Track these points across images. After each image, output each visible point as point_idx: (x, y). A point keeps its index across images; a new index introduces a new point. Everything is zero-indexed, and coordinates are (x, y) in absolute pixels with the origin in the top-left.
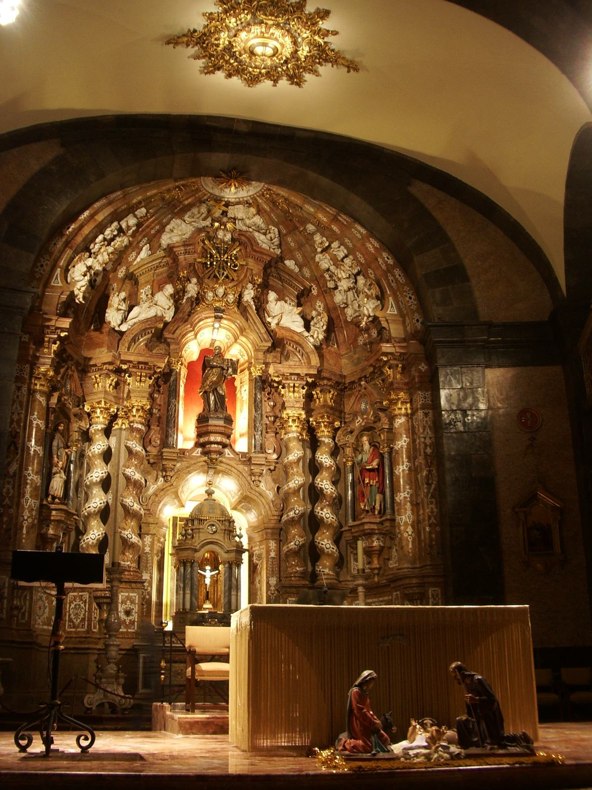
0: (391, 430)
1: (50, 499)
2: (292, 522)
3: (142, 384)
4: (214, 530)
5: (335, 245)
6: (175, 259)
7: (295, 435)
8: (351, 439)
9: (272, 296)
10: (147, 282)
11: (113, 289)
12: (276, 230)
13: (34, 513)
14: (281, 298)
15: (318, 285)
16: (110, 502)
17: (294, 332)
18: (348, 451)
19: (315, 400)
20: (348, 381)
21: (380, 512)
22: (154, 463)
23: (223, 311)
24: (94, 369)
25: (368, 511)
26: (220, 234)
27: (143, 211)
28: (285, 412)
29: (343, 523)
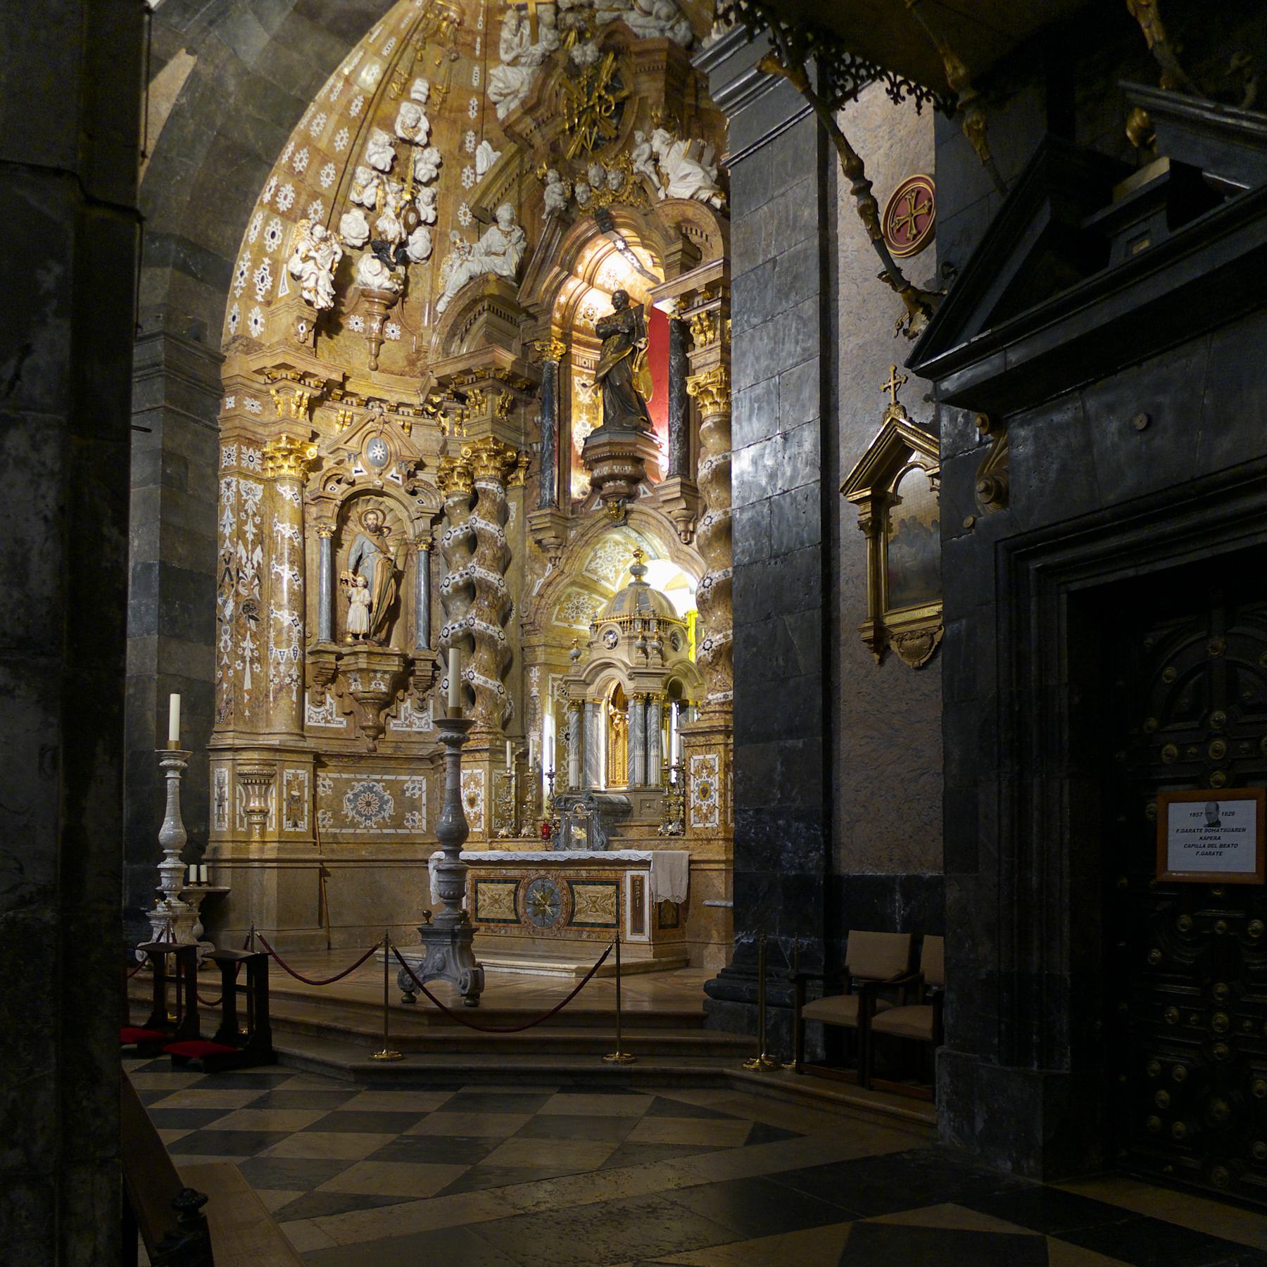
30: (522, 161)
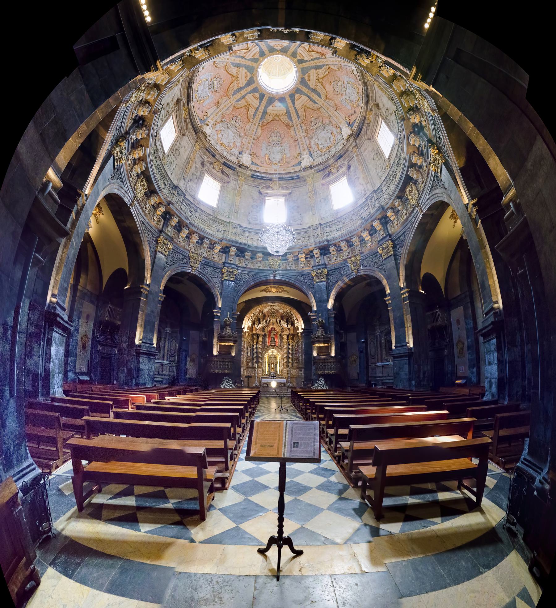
9: (282, 321)
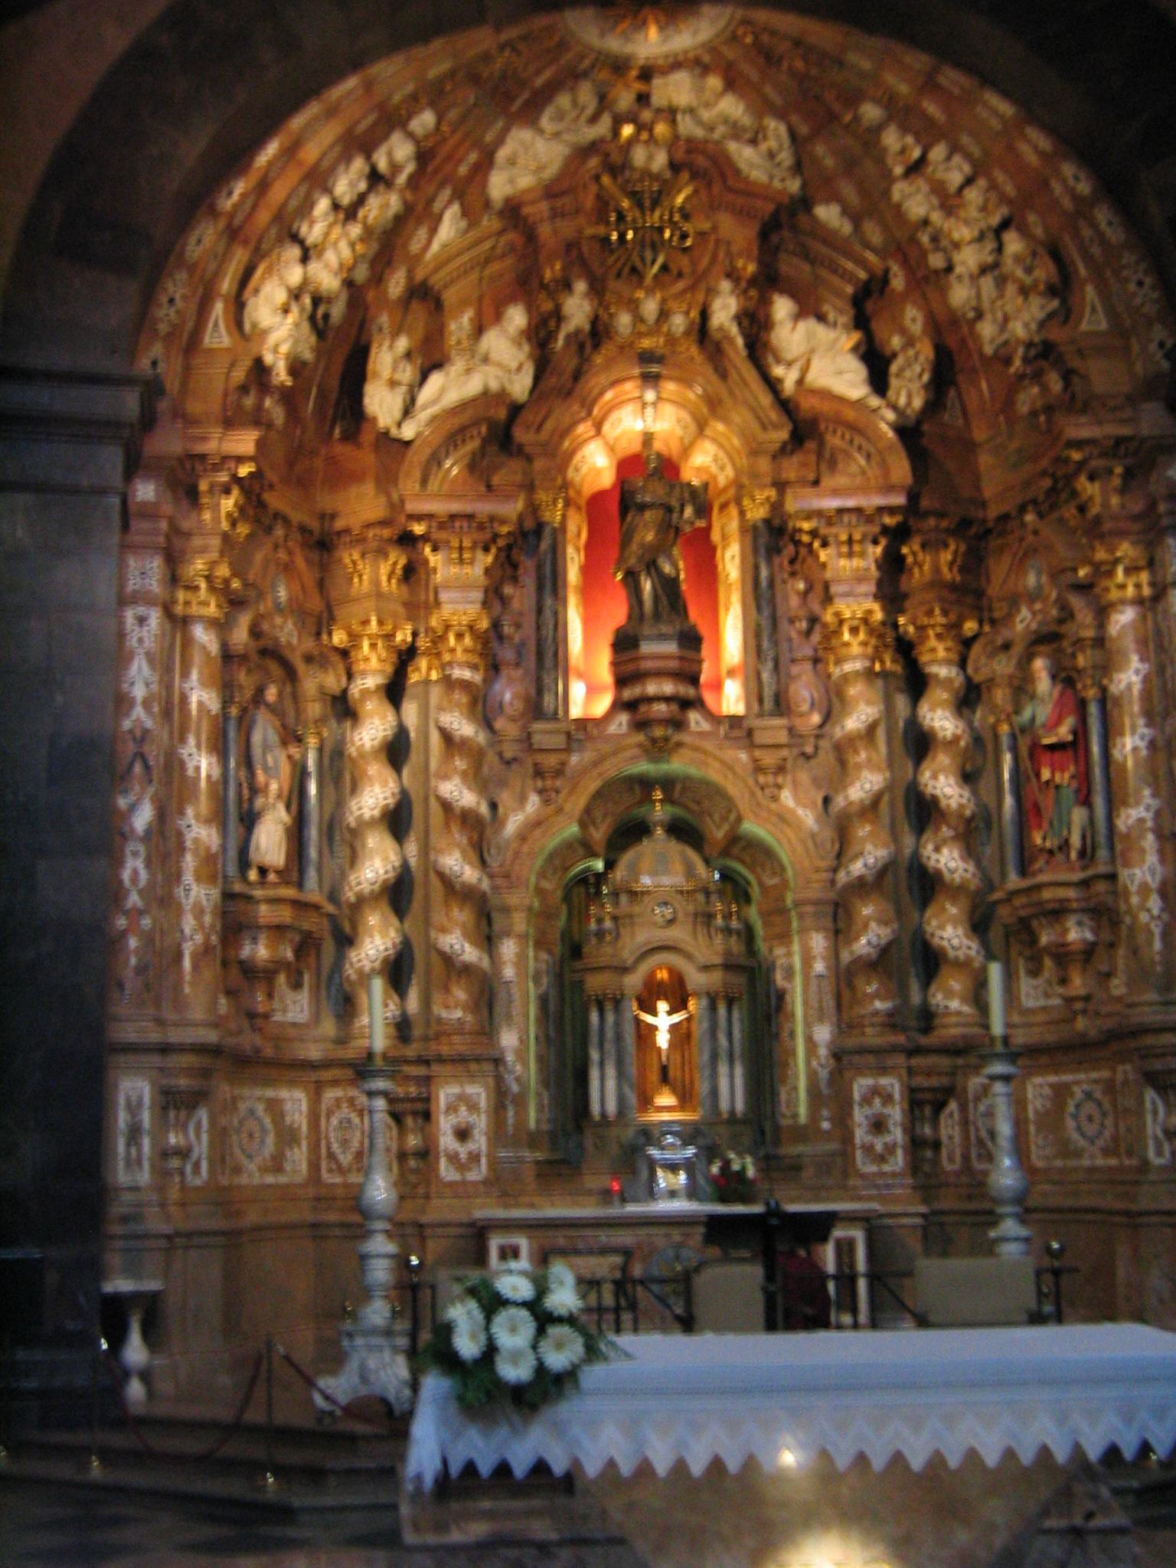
0: (1100, 642)
1: (253, 875)
2: (862, 887)
3: (467, 570)
4: (669, 917)
5: (938, 153)
6: (530, 236)
7: (858, 665)
8: (1003, 667)
9: (782, 307)
10: (463, 304)
11: (380, 329)
12: (783, 129)
13: (208, 919)
14: (809, 308)
15: (905, 263)
16: (413, 862)
17: (841, 400)
18: (1000, 696)
19: (911, 570)
20: (993, 513)
21: (1082, 854)
22: (515, 759)
23: (660, 360)
24: (348, 539)
25: (1051, 852)
26: (639, 156)
27: (424, 122)
28: (830, 611)
29: (995, 876)
30: (497, 241)
